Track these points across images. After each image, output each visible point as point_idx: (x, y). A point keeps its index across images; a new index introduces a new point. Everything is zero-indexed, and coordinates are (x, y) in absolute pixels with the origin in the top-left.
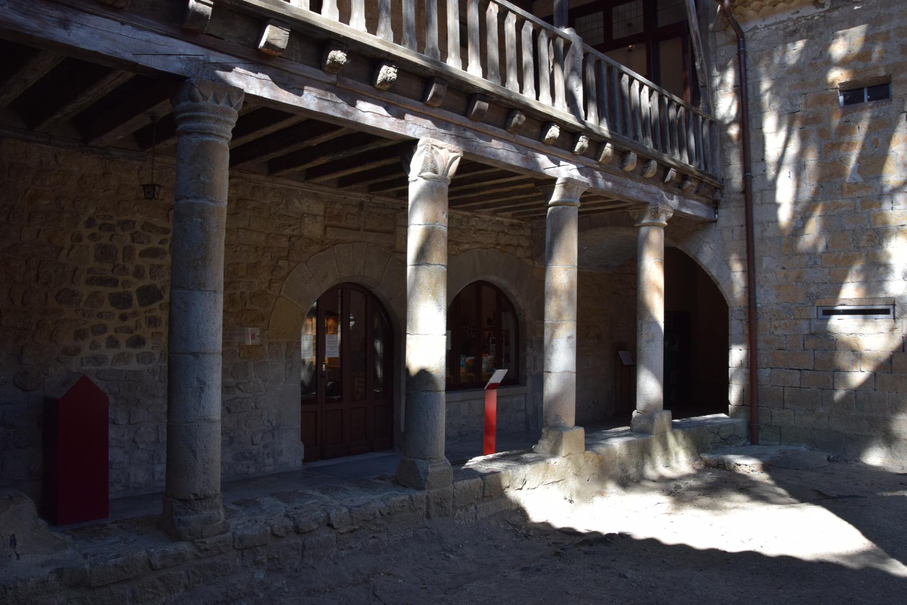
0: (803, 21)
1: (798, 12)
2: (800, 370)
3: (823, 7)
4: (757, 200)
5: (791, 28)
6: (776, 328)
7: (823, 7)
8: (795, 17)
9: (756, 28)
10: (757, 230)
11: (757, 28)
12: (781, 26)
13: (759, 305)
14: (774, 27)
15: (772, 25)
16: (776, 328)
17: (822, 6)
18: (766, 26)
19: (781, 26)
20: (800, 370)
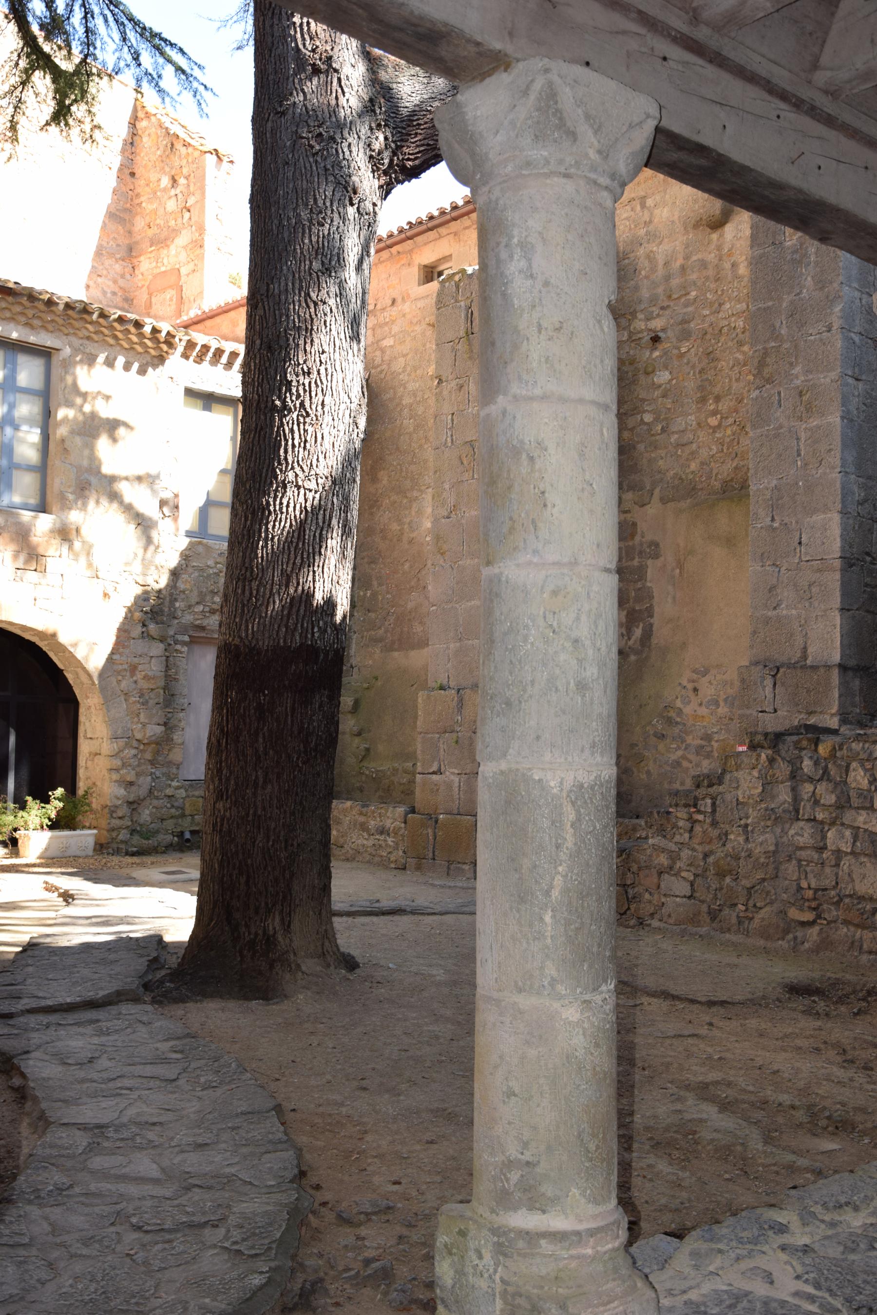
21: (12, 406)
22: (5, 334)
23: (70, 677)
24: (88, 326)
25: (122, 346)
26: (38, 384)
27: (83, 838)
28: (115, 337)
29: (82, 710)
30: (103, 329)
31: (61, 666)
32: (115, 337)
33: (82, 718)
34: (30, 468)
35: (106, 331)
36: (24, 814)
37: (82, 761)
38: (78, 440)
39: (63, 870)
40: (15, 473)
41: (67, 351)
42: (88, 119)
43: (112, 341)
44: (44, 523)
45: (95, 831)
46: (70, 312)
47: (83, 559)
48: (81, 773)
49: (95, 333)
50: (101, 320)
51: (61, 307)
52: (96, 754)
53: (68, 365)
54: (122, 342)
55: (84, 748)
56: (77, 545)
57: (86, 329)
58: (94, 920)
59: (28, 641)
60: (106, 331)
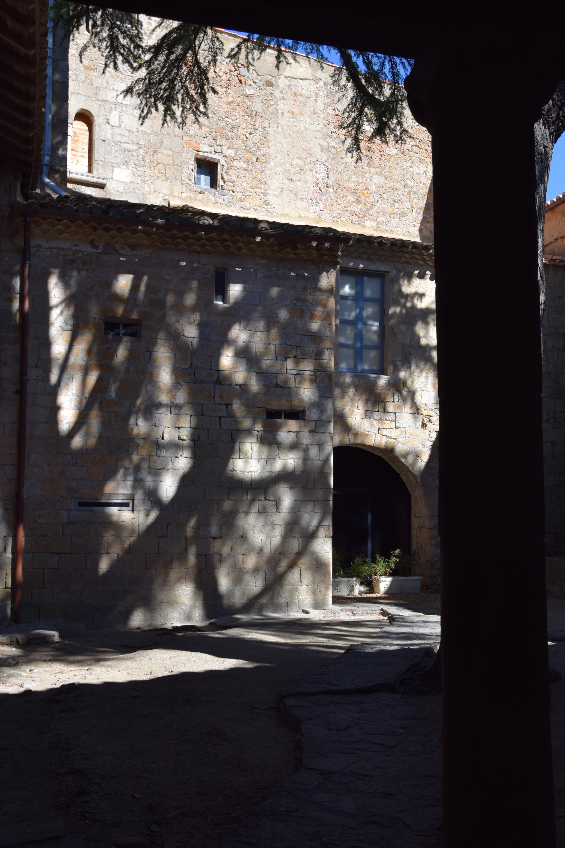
0: (80, 255)
1: (77, 245)
2: (58, 554)
3: (97, 249)
4: (30, 401)
5: (70, 257)
6: (39, 517)
7: (97, 249)
8: (74, 248)
9: (39, 246)
10: (28, 429)
11: (41, 247)
12: (62, 253)
13: (25, 496)
14: (55, 251)
15: (54, 248)
16: (39, 517)
17: (97, 248)
18: (49, 248)
19: (62, 253)
20: (58, 554)
21: (362, 310)
22: (355, 267)
23: (403, 478)
24: (406, 255)
25: (428, 264)
26: (377, 295)
27: (415, 581)
28: (424, 260)
29: (413, 499)
30: (415, 256)
31: (398, 471)
32: (424, 260)
33: (413, 504)
34: (372, 348)
35: (417, 257)
36: (374, 565)
37: (414, 532)
38: (403, 327)
39: (391, 602)
40: (364, 351)
41: (394, 272)
42: (398, 127)
43: (422, 263)
44: (383, 380)
45: (421, 577)
46: (394, 248)
47: (409, 404)
48: (414, 539)
49: (411, 258)
50: (414, 250)
51: (389, 245)
52: (422, 527)
53: (396, 281)
54: (429, 262)
55: (415, 523)
56: (405, 393)
57: (405, 257)
58: (400, 635)
59: (377, 456)
60: (417, 257)
